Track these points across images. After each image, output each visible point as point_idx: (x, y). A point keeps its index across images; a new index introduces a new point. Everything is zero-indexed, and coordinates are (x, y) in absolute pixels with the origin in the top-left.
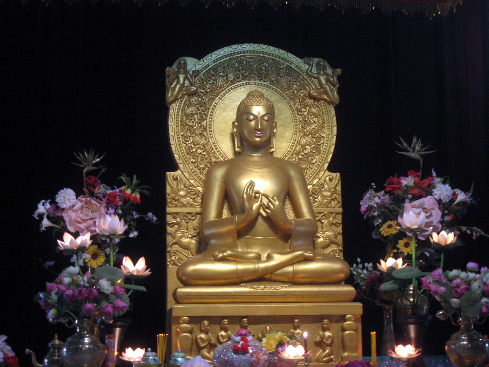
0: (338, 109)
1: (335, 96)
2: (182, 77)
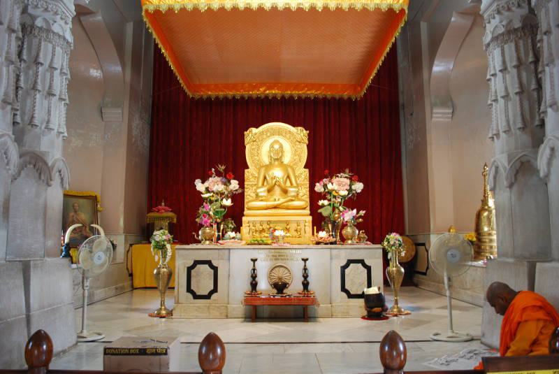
0: (307, 146)
1: (307, 142)
2: (250, 135)
